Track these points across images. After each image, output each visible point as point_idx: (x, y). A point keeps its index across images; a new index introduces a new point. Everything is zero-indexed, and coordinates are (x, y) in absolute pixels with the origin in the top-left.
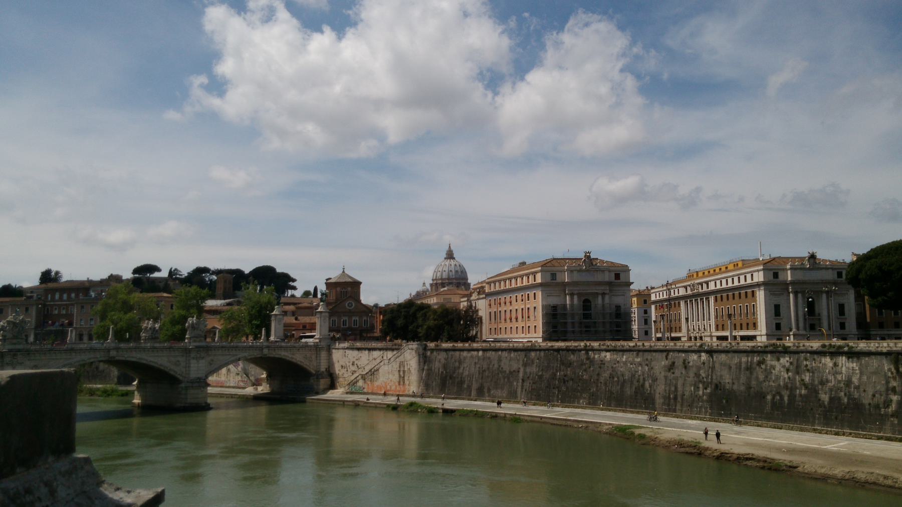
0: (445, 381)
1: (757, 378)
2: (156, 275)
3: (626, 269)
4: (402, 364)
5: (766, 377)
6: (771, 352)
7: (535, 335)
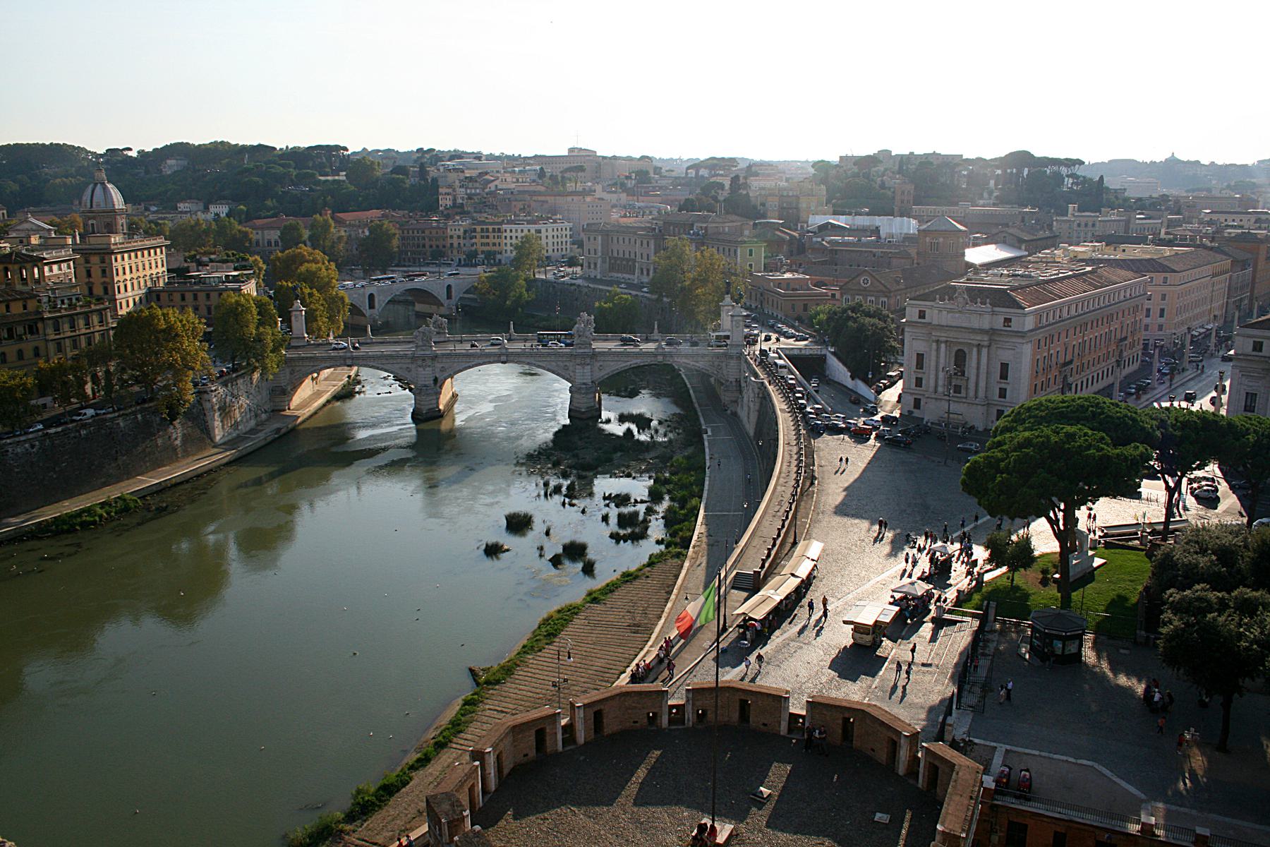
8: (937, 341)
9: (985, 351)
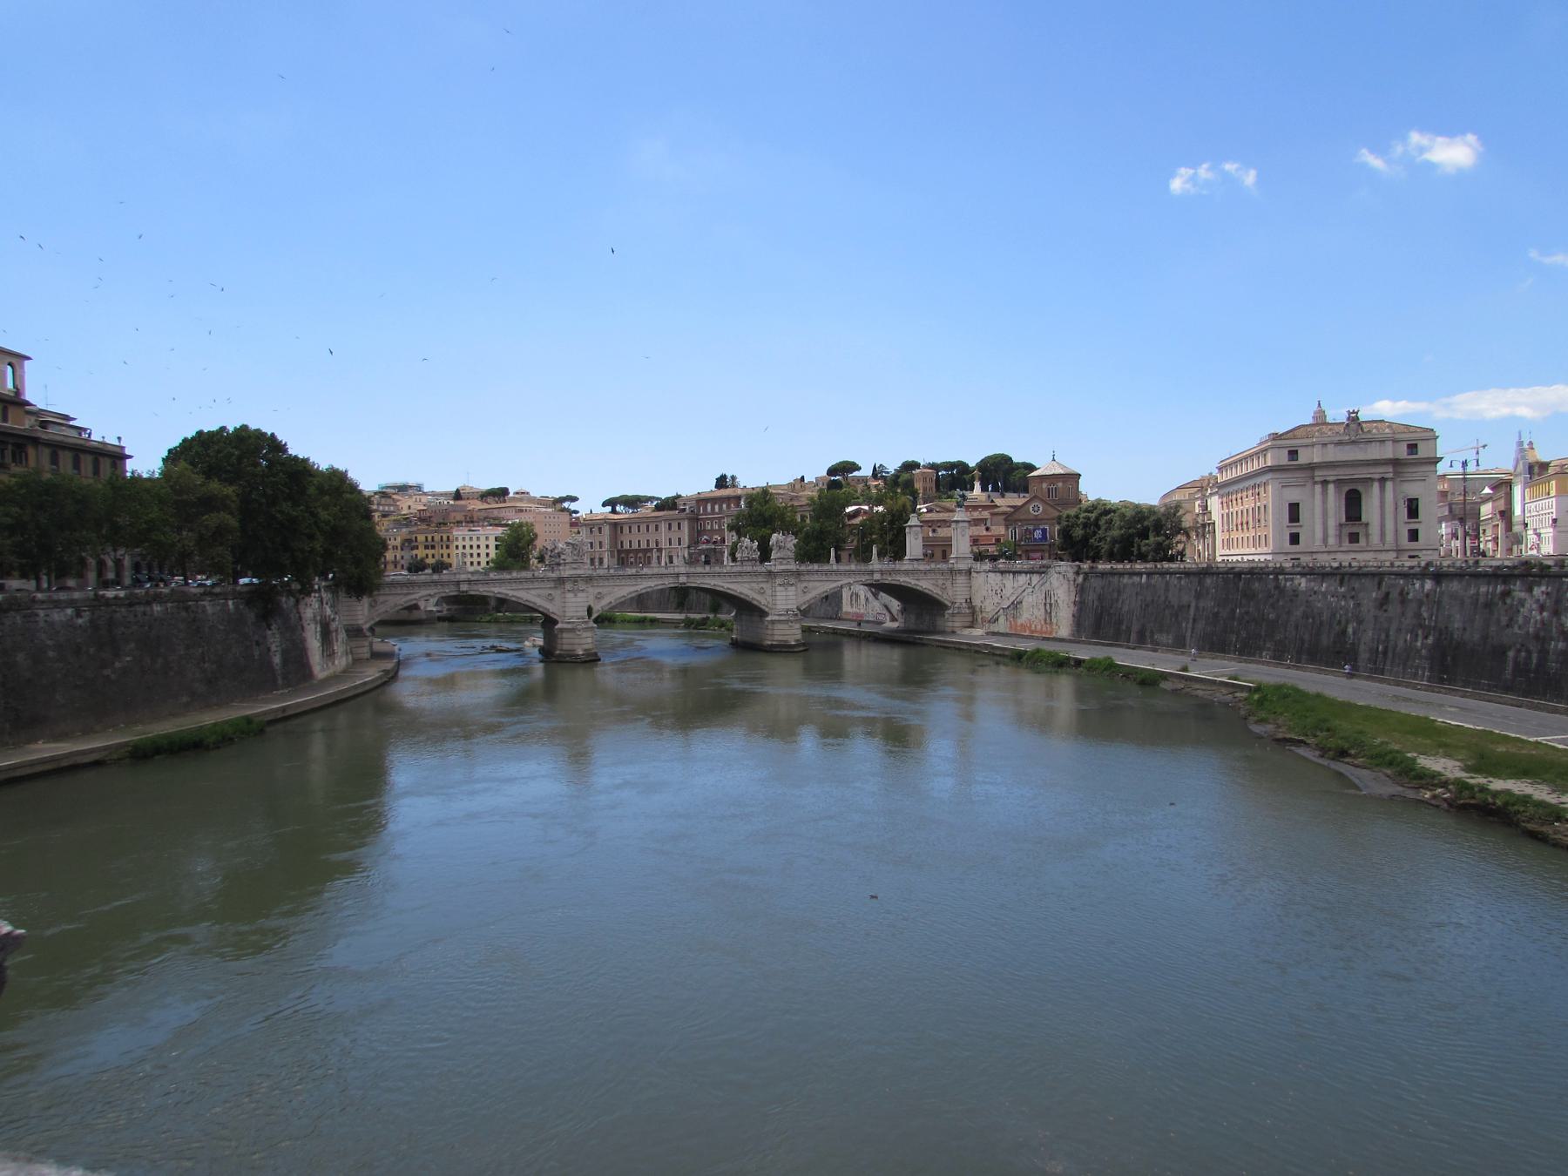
0: (1098, 619)
1: (1498, 621)
2: (856, 474)
3: (1430, 436)
5: (1511, 619)
6: (1522, 576)
7: (1265, 550)
8: (1325, 483)
9: (1389, 485)
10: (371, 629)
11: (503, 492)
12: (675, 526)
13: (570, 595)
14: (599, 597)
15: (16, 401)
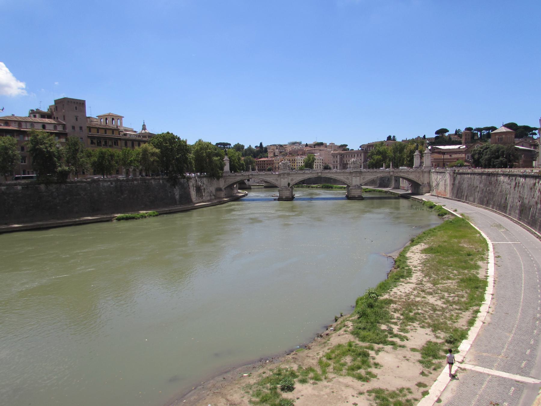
2: (447, 134)
4: (445, 180)
10: (225, 189)
11: (321, 144)
12: (359, 156)
13: (282, 179)
14: (292, 180)
15: (116, 130)
